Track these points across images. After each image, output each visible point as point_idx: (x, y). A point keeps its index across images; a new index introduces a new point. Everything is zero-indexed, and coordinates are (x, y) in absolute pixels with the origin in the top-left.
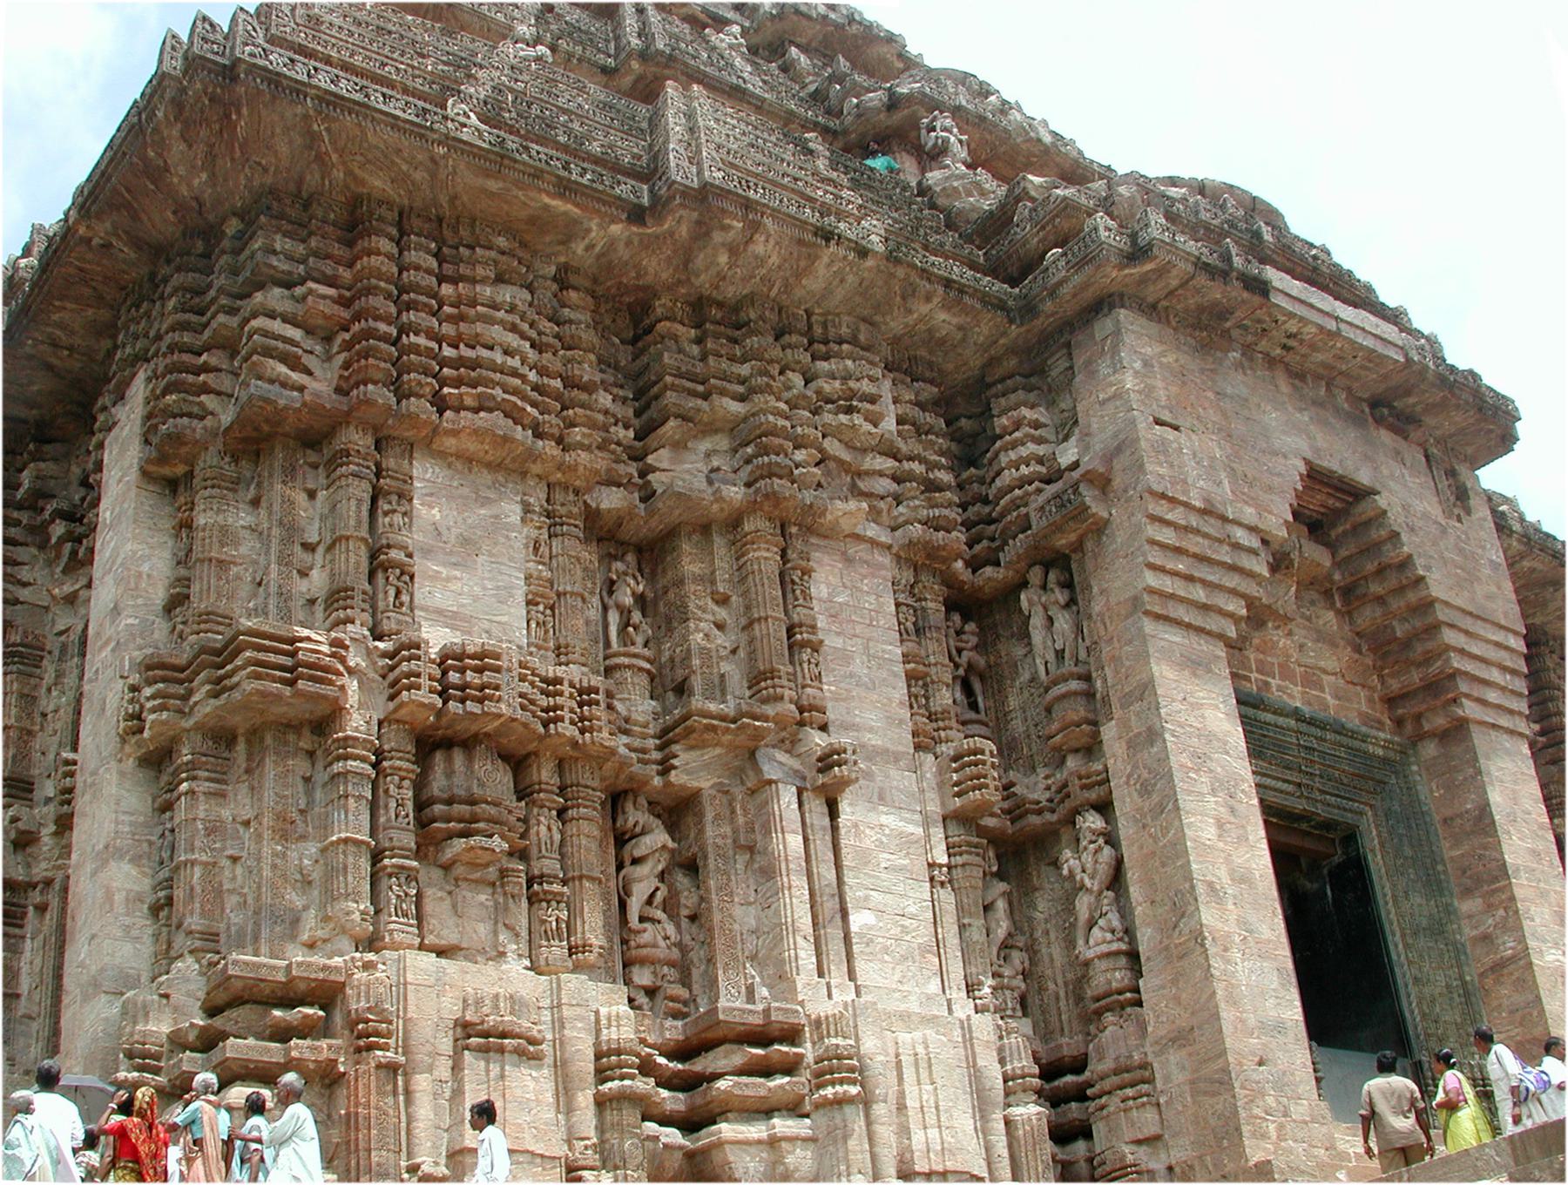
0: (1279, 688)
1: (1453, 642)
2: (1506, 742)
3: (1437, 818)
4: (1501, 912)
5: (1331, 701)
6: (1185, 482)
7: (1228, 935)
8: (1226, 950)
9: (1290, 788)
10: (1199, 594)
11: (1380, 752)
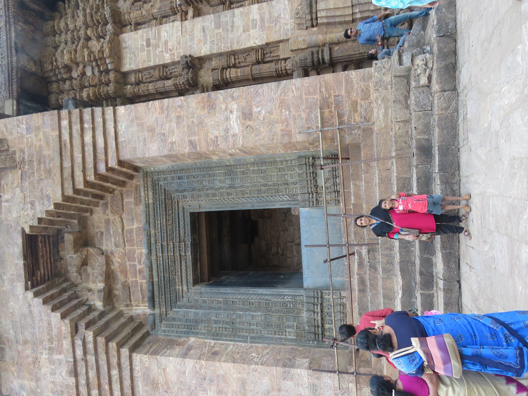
0: (140, 263)
2: (122, 127)
3: (173, 164)
4: (217, 153)
5: (135, 226)
9: (183, 263)
10: (115, 372)
11: (150, 194)
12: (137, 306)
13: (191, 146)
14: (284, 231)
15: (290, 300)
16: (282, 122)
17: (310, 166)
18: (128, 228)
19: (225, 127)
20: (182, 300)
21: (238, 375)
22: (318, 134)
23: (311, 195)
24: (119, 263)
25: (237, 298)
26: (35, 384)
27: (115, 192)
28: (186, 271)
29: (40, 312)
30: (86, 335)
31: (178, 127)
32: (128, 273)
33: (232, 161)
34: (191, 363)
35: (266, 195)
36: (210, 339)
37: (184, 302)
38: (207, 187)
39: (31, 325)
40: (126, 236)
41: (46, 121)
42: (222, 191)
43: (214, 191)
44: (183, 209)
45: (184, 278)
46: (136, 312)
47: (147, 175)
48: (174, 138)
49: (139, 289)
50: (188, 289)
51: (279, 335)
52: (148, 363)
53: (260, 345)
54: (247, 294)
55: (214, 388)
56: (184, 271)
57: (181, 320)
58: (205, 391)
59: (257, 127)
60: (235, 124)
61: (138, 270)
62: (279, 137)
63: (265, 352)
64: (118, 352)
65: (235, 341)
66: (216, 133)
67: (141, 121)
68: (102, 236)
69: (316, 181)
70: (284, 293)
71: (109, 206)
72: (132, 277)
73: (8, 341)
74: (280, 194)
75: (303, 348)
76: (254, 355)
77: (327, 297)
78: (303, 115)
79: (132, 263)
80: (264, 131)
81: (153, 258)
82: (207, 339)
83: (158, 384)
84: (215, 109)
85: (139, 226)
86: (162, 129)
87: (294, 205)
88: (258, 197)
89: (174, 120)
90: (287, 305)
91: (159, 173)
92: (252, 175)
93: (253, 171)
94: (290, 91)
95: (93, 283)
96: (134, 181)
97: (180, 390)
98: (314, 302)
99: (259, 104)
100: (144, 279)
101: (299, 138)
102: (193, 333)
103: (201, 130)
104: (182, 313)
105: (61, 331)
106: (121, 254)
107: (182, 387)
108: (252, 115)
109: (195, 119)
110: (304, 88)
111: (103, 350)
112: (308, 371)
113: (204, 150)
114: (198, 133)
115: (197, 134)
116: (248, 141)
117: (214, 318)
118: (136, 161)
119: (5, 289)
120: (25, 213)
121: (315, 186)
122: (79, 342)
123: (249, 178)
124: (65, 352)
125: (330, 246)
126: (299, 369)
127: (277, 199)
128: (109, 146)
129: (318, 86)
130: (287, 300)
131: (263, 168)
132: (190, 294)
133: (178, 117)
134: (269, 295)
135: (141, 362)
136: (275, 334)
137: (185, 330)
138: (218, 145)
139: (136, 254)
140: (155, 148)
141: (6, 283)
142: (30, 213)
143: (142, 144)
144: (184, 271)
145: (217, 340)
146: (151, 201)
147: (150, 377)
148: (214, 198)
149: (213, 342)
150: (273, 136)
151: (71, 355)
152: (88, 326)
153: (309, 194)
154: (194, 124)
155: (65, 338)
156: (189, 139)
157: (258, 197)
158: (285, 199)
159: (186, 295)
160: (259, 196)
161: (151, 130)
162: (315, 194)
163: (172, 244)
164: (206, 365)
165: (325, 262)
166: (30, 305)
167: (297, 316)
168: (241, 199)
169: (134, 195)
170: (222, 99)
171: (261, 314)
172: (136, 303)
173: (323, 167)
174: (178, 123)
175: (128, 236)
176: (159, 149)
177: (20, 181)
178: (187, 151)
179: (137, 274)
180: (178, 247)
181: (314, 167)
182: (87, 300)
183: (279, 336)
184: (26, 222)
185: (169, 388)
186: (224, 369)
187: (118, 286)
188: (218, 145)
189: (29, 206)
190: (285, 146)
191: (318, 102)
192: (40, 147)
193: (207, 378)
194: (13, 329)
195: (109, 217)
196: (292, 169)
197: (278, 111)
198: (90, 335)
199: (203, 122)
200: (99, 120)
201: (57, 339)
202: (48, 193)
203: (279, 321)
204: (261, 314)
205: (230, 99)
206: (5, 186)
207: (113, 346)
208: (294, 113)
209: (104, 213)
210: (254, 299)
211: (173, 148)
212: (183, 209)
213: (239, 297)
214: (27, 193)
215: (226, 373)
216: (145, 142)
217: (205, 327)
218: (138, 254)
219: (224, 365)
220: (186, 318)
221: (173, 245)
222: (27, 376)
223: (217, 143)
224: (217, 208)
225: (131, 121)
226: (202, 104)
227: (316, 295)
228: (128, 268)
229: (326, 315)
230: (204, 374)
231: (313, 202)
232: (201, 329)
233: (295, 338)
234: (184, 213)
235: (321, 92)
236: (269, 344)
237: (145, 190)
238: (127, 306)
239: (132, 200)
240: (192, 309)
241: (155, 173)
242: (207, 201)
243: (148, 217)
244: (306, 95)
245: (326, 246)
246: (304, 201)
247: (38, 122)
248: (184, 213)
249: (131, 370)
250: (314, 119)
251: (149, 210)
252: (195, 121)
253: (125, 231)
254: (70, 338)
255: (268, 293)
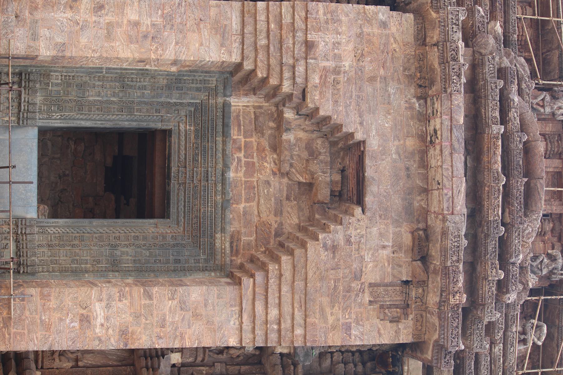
0: (239, 160)
1: (284, 265)
2: (233, 323)
5: (242, 206)
6: (319, 30)
7: (79, 12)
8: (71, 8)
9: (182, 158)
10: (263, 42)
11: (218, 245)
12: (247, 106)
13: (150, 293)
14: (65, 175)
15: (54, 114)
16: (49, 309)
17: (23, 264)
18: (252, 204)
19: (110, 310)
20: (187, 113)
21: (113, 44)
22: (14, 294)
23: (24, 232)
24: (266, 161)
25: (117, 115)
26: (364, 30)
27: (264, 249)
28: (179, 147)
29: (347, 115)
30: (292, 87)
31: (165, 315)
32: (255, 148)
33: (111, 276)
34: (167, 54)
35: (74, 235)
36: (151, 70)
37: (184, 111)
38: (144, 248)
39: (362, 99)
40: (255, 194)
41: (323, 335)
42: (126, 243)
43: (137, 242)
44: (178, 224)
45: (183, 139)
46: (248, 99)
47: (221, 268)
48: (170, 305)
49: (242, 127)
50: (179, 126)
51: (69, 76)
52: (222, 52)
53: (91, 66)
54: (105, 120)
55: (144, 28)
56: (183, 148)
57: (190, 89)
58: (154, 25)
59: (75, 307)
60: (99, 313)
61: (243, 151)
62: (53, 294)
63: (85, 63)
64: (256, 66)
65: (121, 69)
66: (120, 305)
67: (210, 326)
68: (287, 195)
69: (17, 247)
70: (61, 121)
71: (273, 233)
72: (251, 142)
73: (399, 79)
74: (58, 235)
75: (43, 65)
76: (97, 61)
77: (13, 119)
78: (27, 313)
79: (249, 160)
80: (68, 302)
81: (220, 166)
82: (156, 70)
83: (211, 29)
84: (121, 330)
85: (237, 206)
86: (184, 316)
87: (43, 222)
88: (83, 233)
89: (168, 324)
90: (58, 109)
91: (204, 269)
92: (89, 258)
93: (86, 263)
94: (39, 339)
95: (301, 138)
96: (239, 261)
97: (184, 23)
98: (27, 113)
99: (72, 330)
100: (235, 141)
101: (32, 291)
102: (174, 75)
103: (138, 310)
104: (188, 98)
105: (321, 93)
106: (263, 172)
107: (181, 27)
108: (80, 320)
109: (143, 322)
110: (26, 340)
111: (273, 69)
112: (39, 53)
113: (135, 289)
114: (141, 307)
115: (142, 306)
116: (86, 293)
117: (146, 92)
118: (223, 284)
119: (396, 143)
120: (359, 231)
121: (19, 242)
122: (299, 80)
123: (92, 255)
124: (317, 70)
125: (9, 182)
126: (48, 55)
127: (61, 229)
128: (250, 302)
129: (12, 340)
130: (57, 115)
131: (75, 266)
132: (176, 119)
133: (163, 326)
134: (78, 119)
135: (231, 52)
136: (74, 76)
137: (185, 78)
138: (118, 292)
139: (243, 171)
140: (194, 295)
141: (394, 149)
142: (352, 232)
143: (210, 302)
144: (183, 148)
145: (143, 70)
146: (218, 235)
147: (220, 36)
148: (136, 234)
149: (148, 67)
150: (59, 296)
151: (310, 67)
152: (290, 96)
153: (25, 233)
154: (145, 316)
155: (316, 87)
156: (152, 302)
157: (83, 233)
158: (52, 229)
159: (182, 118)
160: (83, 234)
161: (198, 316)
162: (19, 232)
163: (195, 182)
164: (151, 53)
165: (14, 167)
166: (361, 124)
167: (48, 96)
168: (105, 232)
169: (240, 244)
170: (112, 339)
171: (89, 98)
172: (248, 109)
173: (11, 260)
174: (164, 320)
175: (252, 194)
176: (189, 294)
177: (364, 269)
178: (156, 289)
179: (244, 146)
180: (187, 177)
181: (18, 263)
182: (305, 119)
183: (69, 74)
184: (359, 220)
185: (198, 25)
186: (129, 51)
187: (269, 132)
188: (118, 292)
189: (353, 240)
190: (47, 285)
191: (12, 324)
192: (333, 307)
193: (150, 39)
194: (389, 95)
195: (275, 219)
196: (42, 262)
197: (52, 320)
198: (286, 87)
199: (135, 318)
200: (259, 332)
201: (327, 84)
202: (326, 253)
203: (68, 91)
204: (89, 98)
205: (103, 339)
206: (386, 265)
207: (262, 73)
208: (37, 316)
209: (281, 224)
210: (95, 114)
211: (172, 293)
212: (178, 224)
213: (114, 117)
214: (355, 255)
215: (128, 46)
216: (205, 303)
217: (158, 82)
218: (241, 170)
219: (130, 55)
220: (183, 92)
221: (193, 181)
222: (375, 39)
223: (120, 294)
224: (135, 222)
225: (222, 328)
226: (135, 337)
227: (25, 121)
228: (255, 154)
229: (15, 100)
230: (153, 44)
231: (21, 224)
232: (163, 79)
233: (52, 73)
234: (178, 219)
235: (9, 334)
236: (81, 67)
237: (225, 249)
238: (260, 107)
239: (243, 238)
240: (175, 103)
241: (211, 270)
242: (146, 232)
243: (223, 216)
244: (24, 333)
245: (13, 183)
246: (31, 226)
247: (334, 335)
248: (178, 219)
249: (243, 43)
250: (17, 308)
251: (222, 224)
252: (144, 320)
253: (256, 199)
254: (309, 86)
255: (79, 122)
